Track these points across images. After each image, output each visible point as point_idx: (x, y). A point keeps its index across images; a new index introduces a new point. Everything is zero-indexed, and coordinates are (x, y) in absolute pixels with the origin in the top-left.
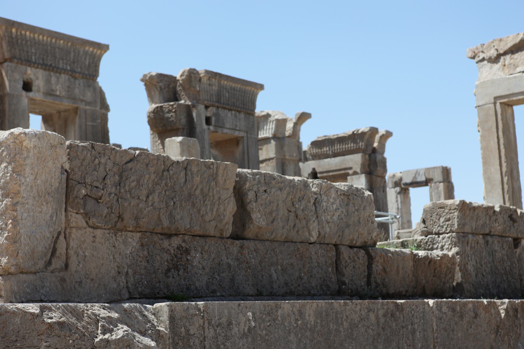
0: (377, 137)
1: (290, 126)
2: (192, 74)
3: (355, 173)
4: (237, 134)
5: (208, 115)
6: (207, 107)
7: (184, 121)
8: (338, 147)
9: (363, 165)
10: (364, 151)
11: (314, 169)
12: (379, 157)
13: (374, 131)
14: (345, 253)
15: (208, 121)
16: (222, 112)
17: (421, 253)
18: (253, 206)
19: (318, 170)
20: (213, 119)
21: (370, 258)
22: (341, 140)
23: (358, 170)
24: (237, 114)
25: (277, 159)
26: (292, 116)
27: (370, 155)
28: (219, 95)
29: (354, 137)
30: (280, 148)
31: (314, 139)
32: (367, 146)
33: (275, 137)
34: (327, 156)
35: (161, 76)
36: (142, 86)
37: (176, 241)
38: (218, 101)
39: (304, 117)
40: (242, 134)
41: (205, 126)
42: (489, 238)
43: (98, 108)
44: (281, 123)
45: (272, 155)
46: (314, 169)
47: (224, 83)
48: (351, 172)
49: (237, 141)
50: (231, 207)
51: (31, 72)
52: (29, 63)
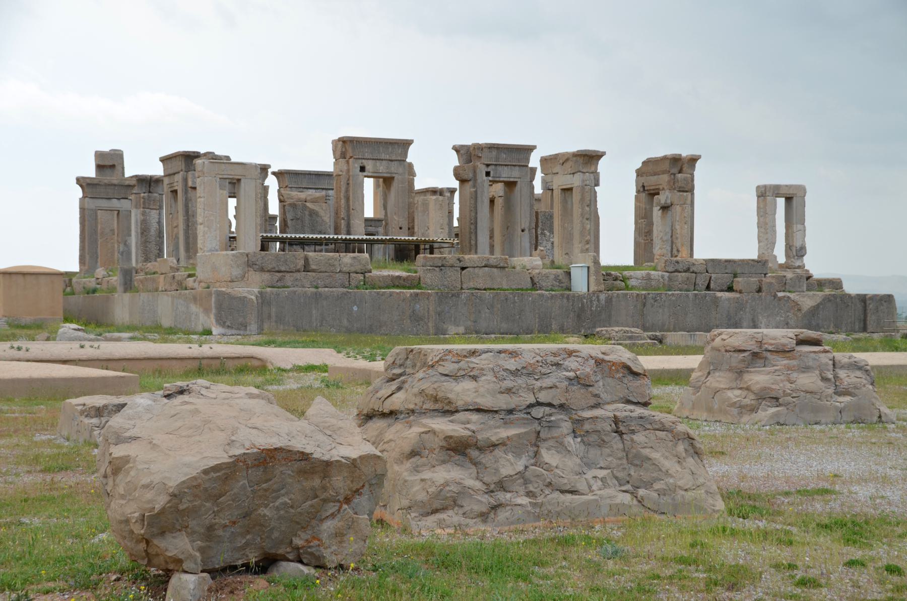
4: (512, 180)
5: (489, 170)
15: (488, 174)
16: (500, 168)
18: (311, 262)
19: (645, 185)
24: (513, 167)
37: (281, 274)
40: (515, 180)
41: (485, 178)
42: (442, 268)
43: (407, 176)
50: (302, 262)
51: (365, 163)
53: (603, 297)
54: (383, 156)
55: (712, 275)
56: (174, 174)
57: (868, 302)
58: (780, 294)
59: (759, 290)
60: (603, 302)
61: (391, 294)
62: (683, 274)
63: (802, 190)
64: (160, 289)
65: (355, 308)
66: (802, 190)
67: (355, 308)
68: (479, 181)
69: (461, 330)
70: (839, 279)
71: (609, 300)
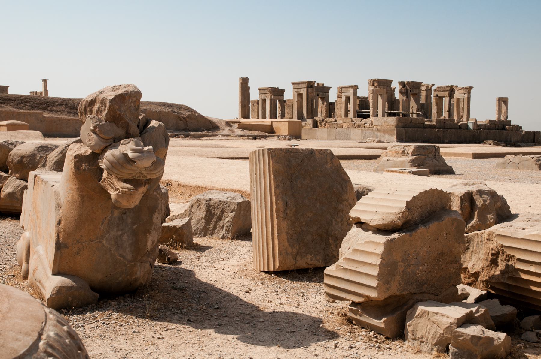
2: (408, 82)
3: (447, 96)
7: (406, 91)
8: (443, 89)
9: (449, 94)
13: (452, 86)
15: (411, 91)
20: (412, 91)
22: (444, 87)
25: (426, 95)
28: (413, 85)
30: (427, 92)
31: (438, 86)
32: (450, 90)
33: (426, 90)
34: (440, 91)
35: (402, 82)
39: (433, 85)
44: (427, 87)
45: (425, 94)
49: (416, 94)
50: (410, 121)
52: (381, 85)
53: (479, 131)
54: (386, 85)
56: (301, 88)
58: (517, 131)
59: (512, 130)
60: (478, 133)
61: (433, 130)
62: (494, 125)
63: (507, 98)
64: (344, 127)
65: (425, 134)
66: (507, 98)
67: (425, 134)
68: (409, 93)
69: (448, 141)
71: (480, 132)
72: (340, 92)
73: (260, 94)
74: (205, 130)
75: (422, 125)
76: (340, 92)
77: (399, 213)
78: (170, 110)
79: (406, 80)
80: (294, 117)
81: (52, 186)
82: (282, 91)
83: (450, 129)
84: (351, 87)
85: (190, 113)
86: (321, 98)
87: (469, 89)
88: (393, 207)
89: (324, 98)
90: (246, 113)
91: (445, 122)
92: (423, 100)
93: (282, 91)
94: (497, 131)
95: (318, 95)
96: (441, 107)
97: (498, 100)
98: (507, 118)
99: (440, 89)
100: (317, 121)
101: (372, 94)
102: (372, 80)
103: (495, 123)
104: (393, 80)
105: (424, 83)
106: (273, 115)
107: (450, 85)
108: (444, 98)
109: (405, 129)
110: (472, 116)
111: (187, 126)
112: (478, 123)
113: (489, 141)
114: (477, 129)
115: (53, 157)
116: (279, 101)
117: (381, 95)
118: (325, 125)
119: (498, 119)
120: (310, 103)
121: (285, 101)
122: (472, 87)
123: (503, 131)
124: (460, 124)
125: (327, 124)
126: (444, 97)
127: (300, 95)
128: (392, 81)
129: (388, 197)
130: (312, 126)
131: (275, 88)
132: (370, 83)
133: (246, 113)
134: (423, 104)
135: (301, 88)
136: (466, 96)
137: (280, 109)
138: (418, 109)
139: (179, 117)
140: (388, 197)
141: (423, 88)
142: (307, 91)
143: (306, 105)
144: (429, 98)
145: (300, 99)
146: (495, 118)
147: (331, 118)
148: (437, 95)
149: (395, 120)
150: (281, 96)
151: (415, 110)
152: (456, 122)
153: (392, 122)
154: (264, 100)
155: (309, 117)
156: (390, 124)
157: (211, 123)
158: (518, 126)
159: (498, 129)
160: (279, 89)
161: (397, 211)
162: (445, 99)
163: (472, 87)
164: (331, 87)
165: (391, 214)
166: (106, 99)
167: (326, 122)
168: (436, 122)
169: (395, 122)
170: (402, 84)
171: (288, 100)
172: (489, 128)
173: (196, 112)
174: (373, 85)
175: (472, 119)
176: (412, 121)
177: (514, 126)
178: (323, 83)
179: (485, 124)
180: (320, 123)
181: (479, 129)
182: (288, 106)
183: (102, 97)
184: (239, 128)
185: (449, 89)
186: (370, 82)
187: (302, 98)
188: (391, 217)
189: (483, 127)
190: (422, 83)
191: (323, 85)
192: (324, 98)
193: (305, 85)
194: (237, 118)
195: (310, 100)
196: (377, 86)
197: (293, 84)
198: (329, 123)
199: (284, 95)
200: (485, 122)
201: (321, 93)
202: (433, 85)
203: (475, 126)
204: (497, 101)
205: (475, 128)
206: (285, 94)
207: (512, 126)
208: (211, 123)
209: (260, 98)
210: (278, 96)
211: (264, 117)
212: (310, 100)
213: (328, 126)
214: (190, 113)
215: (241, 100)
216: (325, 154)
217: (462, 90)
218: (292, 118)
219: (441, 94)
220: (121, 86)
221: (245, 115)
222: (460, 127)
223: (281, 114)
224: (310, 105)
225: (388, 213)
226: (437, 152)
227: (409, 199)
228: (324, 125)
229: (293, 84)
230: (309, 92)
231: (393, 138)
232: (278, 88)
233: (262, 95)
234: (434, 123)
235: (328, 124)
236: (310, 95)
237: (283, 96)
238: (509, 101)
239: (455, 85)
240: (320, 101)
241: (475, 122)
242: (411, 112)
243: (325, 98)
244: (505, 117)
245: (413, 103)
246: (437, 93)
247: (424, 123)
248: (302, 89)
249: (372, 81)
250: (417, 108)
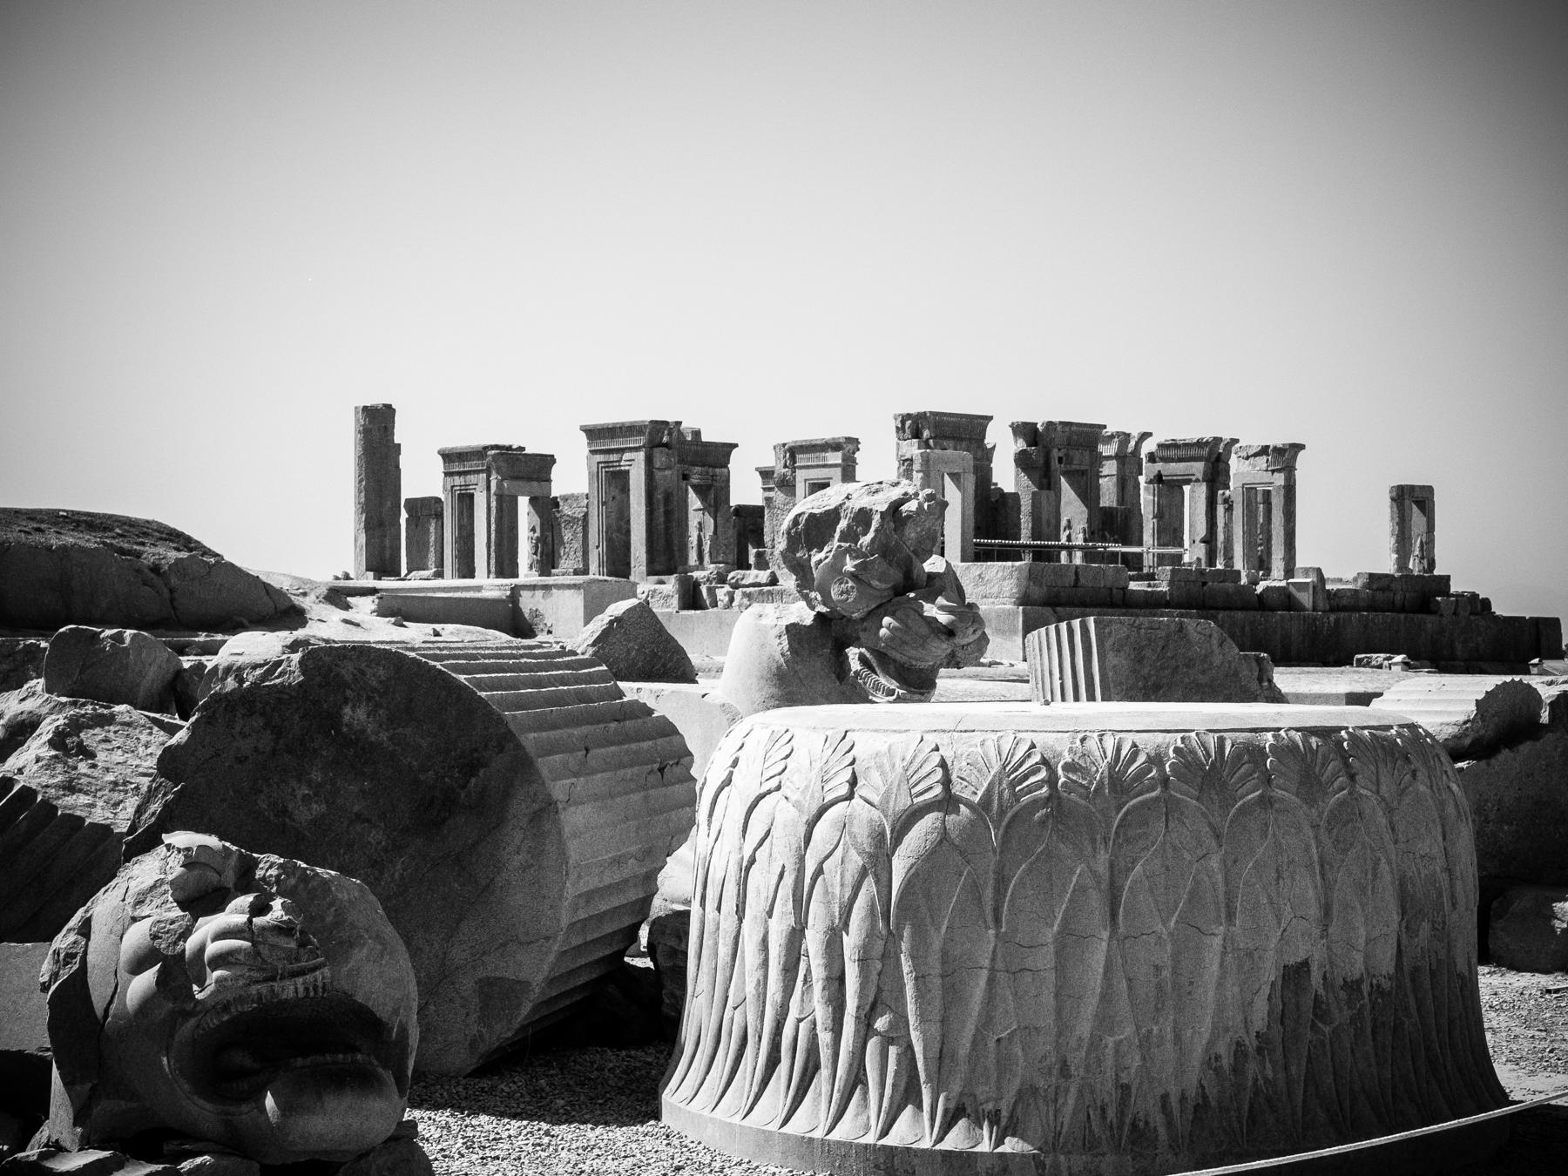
0: (1222, 445)
1: (1133, 443)
3: (1197, 480)
4: (1083, 468)
6: (1060, 450)
7: (1041, 461)
8: (1181, 453)
9: (1205, 473)
10: (1207, 460)
11: (1159, 472)
12: (1221, 466)
13: (1217, 440)
14: (1114, 590)
15: (1060, 460)
17: (1150, 589)
21: (1124, 594)
22: (1187, 445)
23: (1200, 478)
26: (1135, 434)
27: (1213, 463)
28: (1069, 439)
29: (1200, 444)
31: (1162, 441)
35: (1025, 424)
36: (1010, 429)
38: (1069, 444)
39: (1145, 436)
41: (1057, 465)
45: (1115, 473)
46: (1159, 472)
47: (1074, 428)
48: (1194, 478)
49: (1083, 473)
50: (1073, 578)
52: (946, 438)
55: (1407, 595)
56: (622, 451)
57: (1541, 627)
59: (1455, 614)
66: (1430, 490)
68: (1053, 468)
70: (1487, 599)
71: (1337, 621)
72: (785, 466)
73: (447, 474)
74: (245, 621)
75: (1117, 595)
76: (785, 466)
77: (1465, 723)
78: (90, 541)
79: (1040, 420)
80: (593, 567)
81: (703, 696)
82: (548, 461)
83: (1225, 609)
84: (835, 446)
85: (184, 555)
86: (697, 489)
87: (1285, 457)
88: (1450, 713)
89: (709, 487)
90: (388, 554)
91: (1204, 584)
92: (1108, 496)
93: (548, 461)
94: (1402, 616)
95: (685, 477)
96: (1177, 525)
97: (1394, 494)
98: (1432, 564)
99: (1172, 453)
100: (697, 585)
101: (921, 475)
102: (909, 416)
103: (1393, 585)
104: (991, 418)
105: (1110, 430)
106: (505, 565)
107: (1208, 435)
108: (1186, 489)
109: (1059, 609)
110: (1301, 562)
111: (174, 608)
112: (1328, 587)
113: (1375, 656)
114: (1328, 607)
115: (585, 645)
116: (534, 501)
117: (955, 477)
118: (732, 600)
119: (1400, 569)
120: (662, 510)
121: (555, 503)
122: (1298, 447)
123: (1424, 616)
124: (1260, 588)
125: (738, 594)
126: (1188, 482)
127: (616, 480)
128: (991, 418)
129: (1430, 697)
130: (675, 601)
131: (509, 448)
132: (900, 430)
133: (388, 554)
134: (1108, 513)
135: (622, 451)
136: (1279, 479)
137: (538, 534)
138: (1093, 533)
139: (139, 571)
140: (1430, 697)
141: (1108, 450)
142: (649, 460)
143: (643, 518)
144: (1130, 487)
145: (615, 492)
146: (1386, 564)
147: (748, 567)
148: (1159, 478)
149: (1015, 574)
150: (539, 480)
151: (1081, 536)
152: (1244, 581)
153: (1005, 583)
154: (465, 501)
155: (658, 567)
156: (995, 590)
157: (268, 593)
158: (1474, 596)
159: (1403, 609)
160: (527, 451)
161: (1462, 718)
162: (1192, 491)
163: (1301, 447)
164: (736, 446)
165: (1448, 724)
166: (871, 510)
167: (736, 586)
168: (1171, 583)
169: (1014, 581)
170: (1025, 431)
171: (565, 498)
172: (1372, 607)
173: (207, 552)
174: (917, 434)
175: (1306, 571)
176: (1082, 581)
177: (1460, 596)
178: (696, 426)
179: (1356, 591)
180: (711, 591)
181: (1332, 610)
182: (573, 520)
183: (857, 507)
184: (382, 612)
185: (1205, 452)
186: (903, 422)
187: (625, 489)
188: (1450, 730)
189: (1345, 602)
190: (1105, 427)
191: (697, 434)
192: (709, 487)
193: (641, 441)
194: (347, 577)
195: (659, 496)
196: (931, 442)
197: (593, 433)
198: (748, 590)
199: (553, 476)
200: (1355, 580)
201: (700, 469)
202: (1145, 436)
203: (1320, 596)
204: (1393, 499)
205: (1321, 604)
206: (556, 473)
207: (1453, 595)
208: (268, 593)
209: (445, 489)
210: (530, 479)
211: (467, 570)
212: (659, 496)
213: (746, 601)
214: (184, 555)
215: (363, 500)
216: (1208, 632)
217: (1264, 458)
218: (585, 572)
219: (1174, 469)
220: (881, 483)
221: (382, 563)
222: (1263, 603)
223: (542, 553)
224: (662, 519)
225: (1442, 724)
226: (1265, 679)
227: (1480, 697)
228: (726, 599)
229: (593, 433)
230: (658, 464)
231: (1008, 644)
232: (523, 449)
233: (458, 480)
234: (1164, 587)
235: (745, 595)
236: (658, 475)
237: (549, 480)
238: (1437, 499)
239: (1227, 436)
240: (694, 501)
241: (1315, 579)
242: (1063, 540)
243: (712, 491)
244: (1425, 562)
245: (1072, 509)
246: (1159, 466)
247: (1125, 589)
248: (627, 456)
249: (908, 423)
250: (1086, 526)
